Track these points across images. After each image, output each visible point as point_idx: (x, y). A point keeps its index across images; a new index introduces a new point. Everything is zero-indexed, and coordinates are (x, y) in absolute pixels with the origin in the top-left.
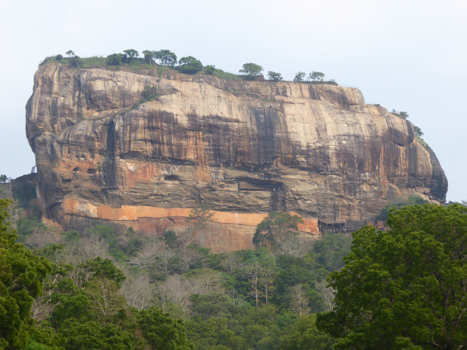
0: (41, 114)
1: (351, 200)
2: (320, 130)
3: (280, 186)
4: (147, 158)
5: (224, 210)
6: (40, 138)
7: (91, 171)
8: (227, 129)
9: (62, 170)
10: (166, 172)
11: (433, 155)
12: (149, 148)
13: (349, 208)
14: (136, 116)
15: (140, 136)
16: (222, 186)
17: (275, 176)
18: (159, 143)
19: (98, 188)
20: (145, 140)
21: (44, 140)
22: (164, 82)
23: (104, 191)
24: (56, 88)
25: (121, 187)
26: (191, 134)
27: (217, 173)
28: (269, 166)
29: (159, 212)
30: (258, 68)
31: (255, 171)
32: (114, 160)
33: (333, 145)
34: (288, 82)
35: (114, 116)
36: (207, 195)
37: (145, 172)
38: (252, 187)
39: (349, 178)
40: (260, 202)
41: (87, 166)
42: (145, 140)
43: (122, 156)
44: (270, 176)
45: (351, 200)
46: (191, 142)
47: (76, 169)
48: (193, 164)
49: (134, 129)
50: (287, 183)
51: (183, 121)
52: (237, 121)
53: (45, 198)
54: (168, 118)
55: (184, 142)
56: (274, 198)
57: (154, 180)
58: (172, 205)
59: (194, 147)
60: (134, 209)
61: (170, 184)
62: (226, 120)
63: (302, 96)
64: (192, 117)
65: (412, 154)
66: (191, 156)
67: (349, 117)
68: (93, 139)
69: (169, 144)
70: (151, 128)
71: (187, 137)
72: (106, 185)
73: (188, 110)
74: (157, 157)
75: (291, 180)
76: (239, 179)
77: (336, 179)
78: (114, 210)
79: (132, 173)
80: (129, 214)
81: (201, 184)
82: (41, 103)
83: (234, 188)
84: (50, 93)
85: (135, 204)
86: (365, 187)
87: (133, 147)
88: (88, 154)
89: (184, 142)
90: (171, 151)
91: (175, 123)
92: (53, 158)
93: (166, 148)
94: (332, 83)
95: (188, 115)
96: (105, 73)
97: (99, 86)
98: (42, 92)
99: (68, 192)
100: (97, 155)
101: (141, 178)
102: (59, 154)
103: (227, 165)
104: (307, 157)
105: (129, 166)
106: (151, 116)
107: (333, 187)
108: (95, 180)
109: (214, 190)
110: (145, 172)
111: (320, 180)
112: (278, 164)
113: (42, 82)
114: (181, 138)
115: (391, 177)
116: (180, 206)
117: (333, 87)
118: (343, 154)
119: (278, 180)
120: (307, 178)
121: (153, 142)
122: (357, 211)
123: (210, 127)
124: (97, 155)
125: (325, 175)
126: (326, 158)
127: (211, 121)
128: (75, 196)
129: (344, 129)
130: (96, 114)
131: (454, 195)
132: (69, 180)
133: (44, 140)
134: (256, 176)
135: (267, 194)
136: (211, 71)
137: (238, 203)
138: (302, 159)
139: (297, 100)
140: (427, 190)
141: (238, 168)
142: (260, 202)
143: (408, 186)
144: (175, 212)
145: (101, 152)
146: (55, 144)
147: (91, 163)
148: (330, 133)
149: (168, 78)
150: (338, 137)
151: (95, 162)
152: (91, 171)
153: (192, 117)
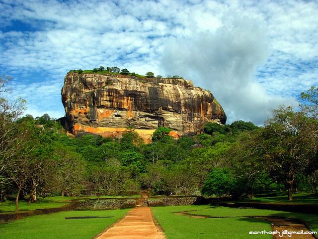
0: (66, 92)
1: (190, 124)
2: (178, 96)
3: (162, 119)
4: (107, 108)
5: (139, 129)
6: (66, 102)
7: (85, 113)
8: (140, 95)
9: (74, 113)
10: (116, 114)
11: (221, 107)
12: (108, 104)
13: (190, 127)
14: (103, 91)
15: (105, 99)
16: (138, 119)
17: (159, 115)
18: (112, 102)
19: (88, 120)
20: (107, 101)
21: (68, 102)
22: (114, 78)
23: (91, 121)
24: (72, 83)
25: (97, 120)
26: (125, 98)
27: (136, 114)
28: (157, 110)
29: (112, 130)
30: (153, 74)
31: (151, 113)
32: (94, 110)
33: (182, 101)
34: (164, 78)
35: (94, 91)
36: (132, 122)
37: (107, 114)
38: (150, 119)
39: (189, 115)
40: (154, 125)
41: (84, 112)
42: (107, 101)
43: (98, 107)
44: (157, 114)
45: (190, 124)
46: (125, 101)
47: (80, 113)
48: (126, 110)
49: (102, 96)
50: (164, 117)
51: (122, 93)
52: (144, 92)
53: (68, 125)
54: (116, 91)
55: (122, 101)
56: (160, 123)
57: (111, 117)
58: (118, 127)
59: (127, 102)
60: (102, 128)
61: (117, 118)
62: (139, 92)
63: (170, 84)
64: (126, 91)
65: (214, 106)
66: (125, 107)
67: (188, 91)
68: (86, 100)
69: (117, 102)
70: (109, 95)
71: (124, 99)
72: (91, 120)
73: (124, 88)
74: (112, 107)
75: (166, 116)
76: (145, 116)
77: (185, 116)
78: (95, 129)
79: (102, 114)
80: (102, 131)
81: (130, 118)
82: (66, 88)
83: (143, 120)
84: (70, 84)
85: (103, 126)
86: (195, 119)
87: (102, 103)
88: (84, 107)
89: (122, 101)
90: (117, 105)
91: (119, 93)
92: (70, 109)
93: (115, 103)
94: (181, 78)
95: (124, 90)
96: (91, 75)
97: (89, 79)
98: (67, 84)
99: (77, 122)
100: (88, 107)
101: (105, 116)
102: (73, 107)
103: (140, 110)
104: (172, 107)
105: (101, 111)
106: (109, 91)
107: (183, 118)
108: (87, 117)
109: (135, 120)
110: (107, 114)
111: (178, 116)
112: (161, 109)
113: (68, 80)
114: (121, 99)
115: (205, 115)
116: (121, 127)
117: (182, 80)
118: (186, 105)
119: (161, 116)
120: (173, 115)
121: (111, 101)
122: (193, 128)
123: (133, 95)
124: (88, 107)
125: (180, 114)
126: (180, 107)
127: (133, 92)
128: (79, 124)
129: (187, 96)
130: (88, 91)
131: (229, 122)
132: (77, 118)
133: (68, 102)
134: (152, 115)
135: (157, 122)
136: (134, 74)
137: (145, 126)
138: (170, 107)
139: (167, 85)
140: (219, 120)
141: (145, 112)
142: (154, 125)
143: (212, 119)
144: (119, 130)
145: (89, 106)
146: (72, 103)
147: (85, 110)
148: (182, 97)
149: (116, 77)
150: (185, 99)
151: (87, 110)
152: (85, 113)
153: (126, 91)
